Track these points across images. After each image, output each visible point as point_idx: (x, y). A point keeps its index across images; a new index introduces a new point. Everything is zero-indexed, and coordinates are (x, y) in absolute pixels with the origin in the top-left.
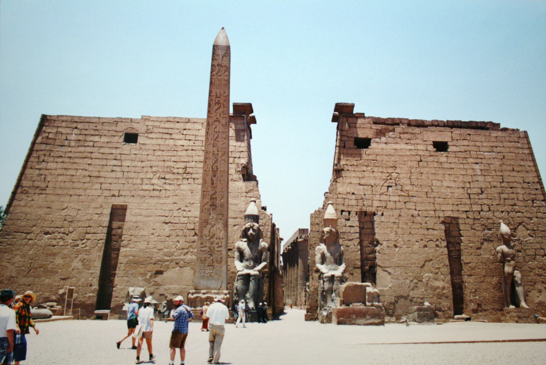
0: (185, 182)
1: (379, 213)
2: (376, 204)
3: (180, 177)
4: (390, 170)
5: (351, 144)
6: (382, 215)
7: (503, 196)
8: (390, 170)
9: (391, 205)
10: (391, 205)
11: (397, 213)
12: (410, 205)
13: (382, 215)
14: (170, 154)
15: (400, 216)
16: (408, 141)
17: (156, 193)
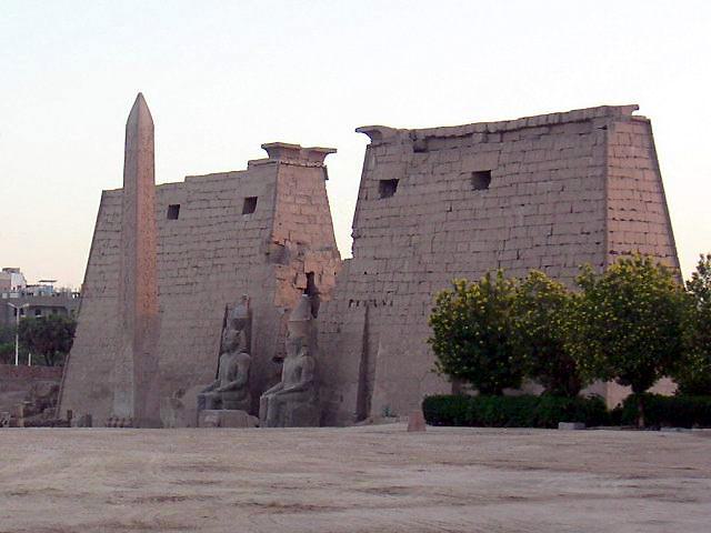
0: (214, 271)
1: (388, 303)
2: (387, 287)
3: (209, 263)
4: (412, 231)
5: (375, 192)
6: (391, 304)
7: (546, 262)
8: (412, 231)
9: (403, 288)
10: (403, 288)
11: (407, 299)
12: (425, 287)
13: (391, 304)
14: (207, 229)
15: (410, 305)
16: (441, 178)
17: (188, 288)
